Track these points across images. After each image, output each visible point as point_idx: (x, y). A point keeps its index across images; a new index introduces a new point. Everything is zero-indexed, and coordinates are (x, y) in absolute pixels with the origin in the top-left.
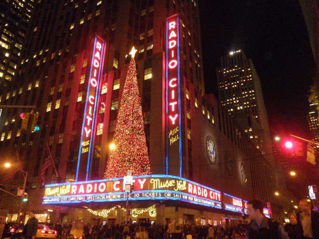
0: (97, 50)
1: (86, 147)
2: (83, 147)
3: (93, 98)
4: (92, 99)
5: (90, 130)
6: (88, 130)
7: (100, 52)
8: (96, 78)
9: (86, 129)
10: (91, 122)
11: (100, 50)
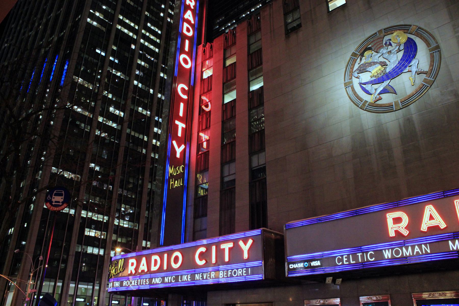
1: (176, 178)
3: (186, 88)
4: (183, 89)
5: (183, 147)
6: (179, 147)
7: (193, 11)
8: (189, 54)
9: (174, 143)
11: (192, 8)
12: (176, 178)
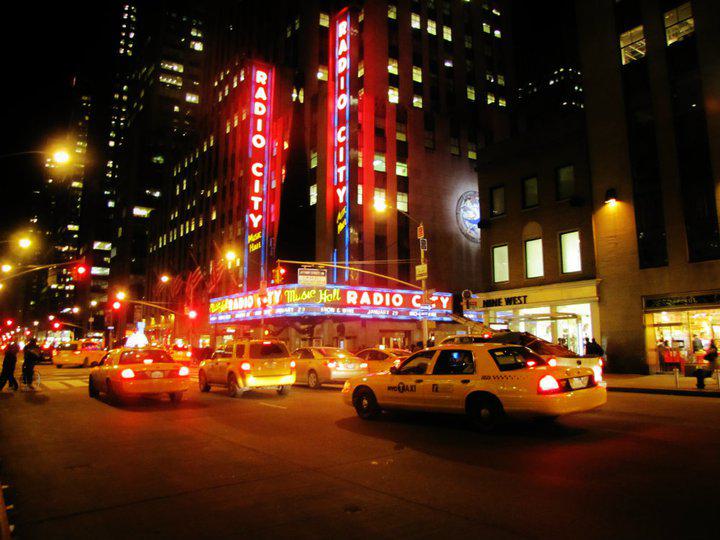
0: (260, 85)
1: (255, 242)
2: (251, 243)
3: (260, 166)
5: (260, 217)
10: (261, 204)
12: (255, 242)
